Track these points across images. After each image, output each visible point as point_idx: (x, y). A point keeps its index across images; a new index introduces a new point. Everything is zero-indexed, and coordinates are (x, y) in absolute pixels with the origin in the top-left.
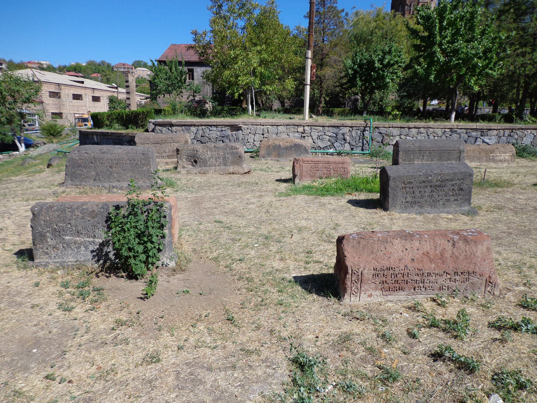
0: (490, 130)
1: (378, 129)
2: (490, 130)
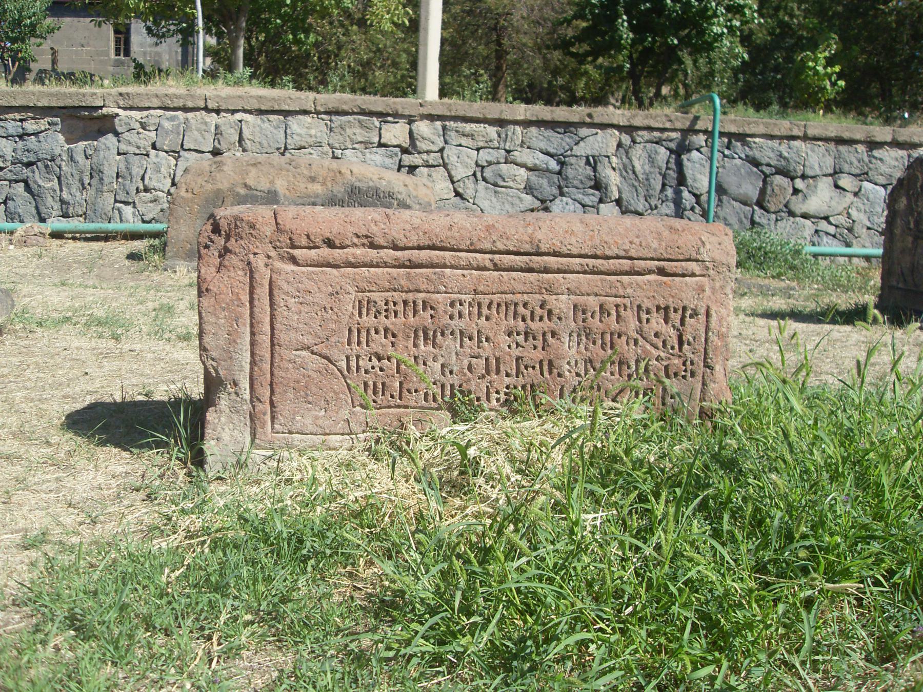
1: (745, 143)
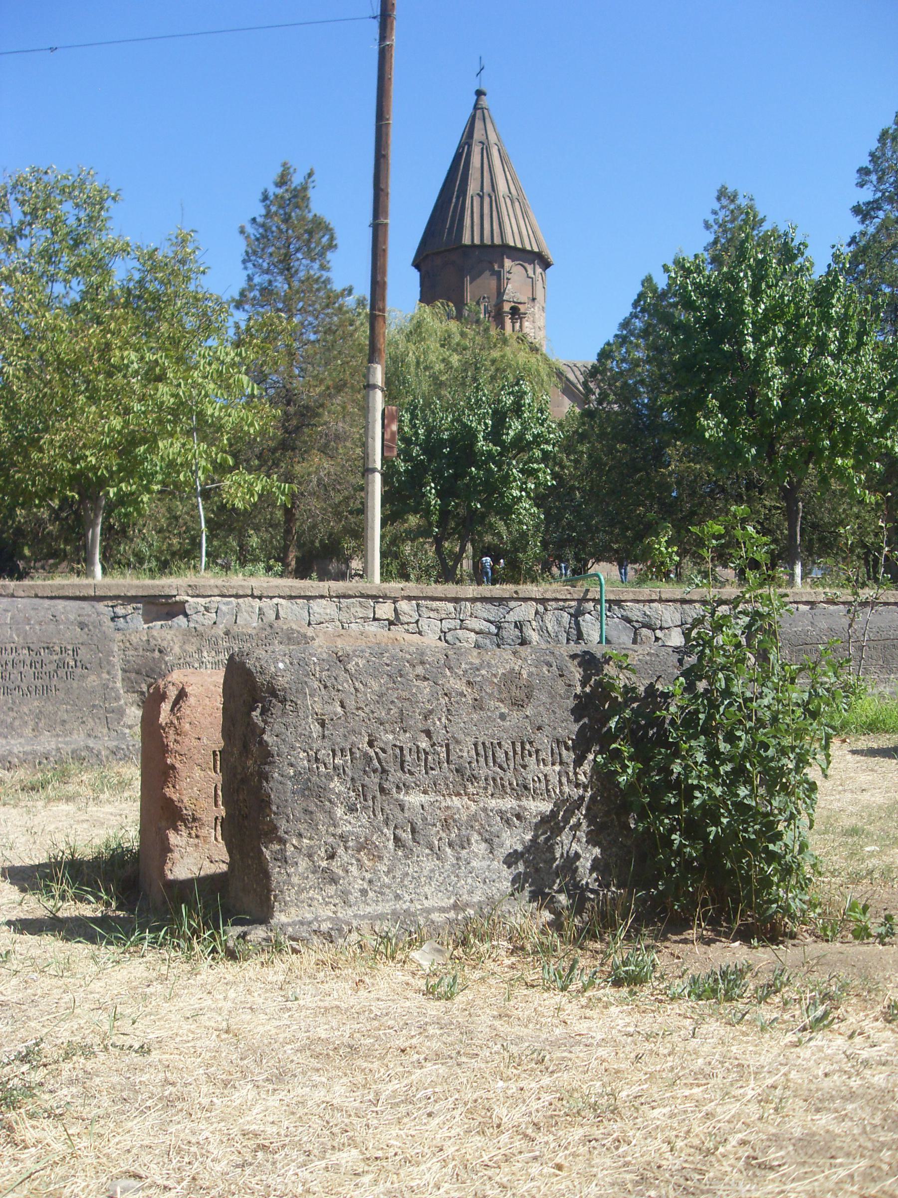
1: (620, 607)
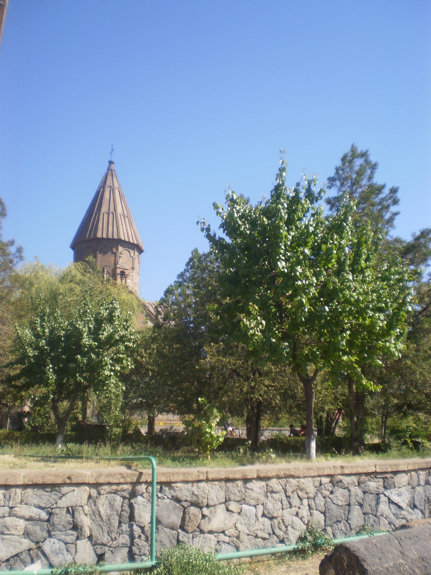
0: (396, 473)
1: (171, 488)
2: (396, 473)
